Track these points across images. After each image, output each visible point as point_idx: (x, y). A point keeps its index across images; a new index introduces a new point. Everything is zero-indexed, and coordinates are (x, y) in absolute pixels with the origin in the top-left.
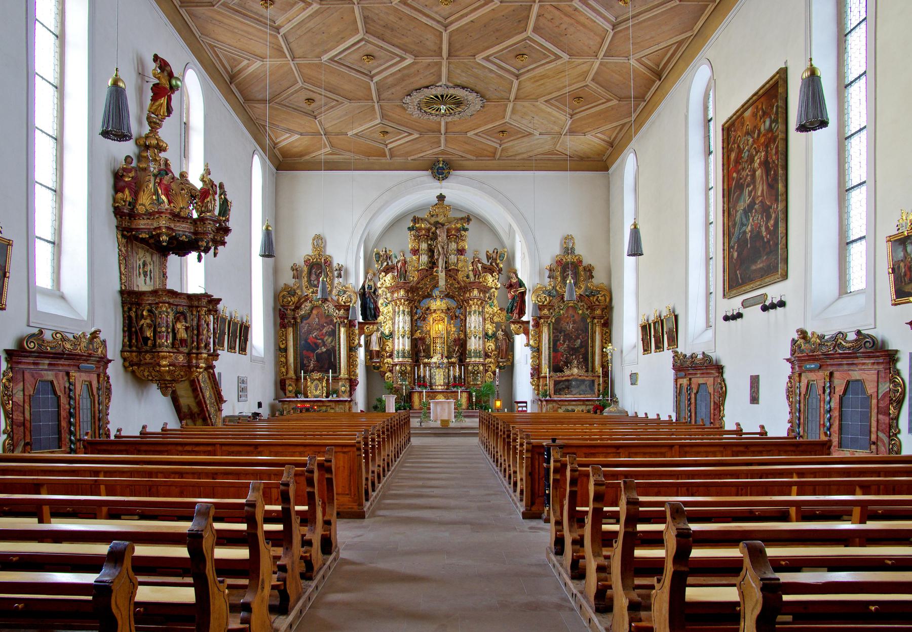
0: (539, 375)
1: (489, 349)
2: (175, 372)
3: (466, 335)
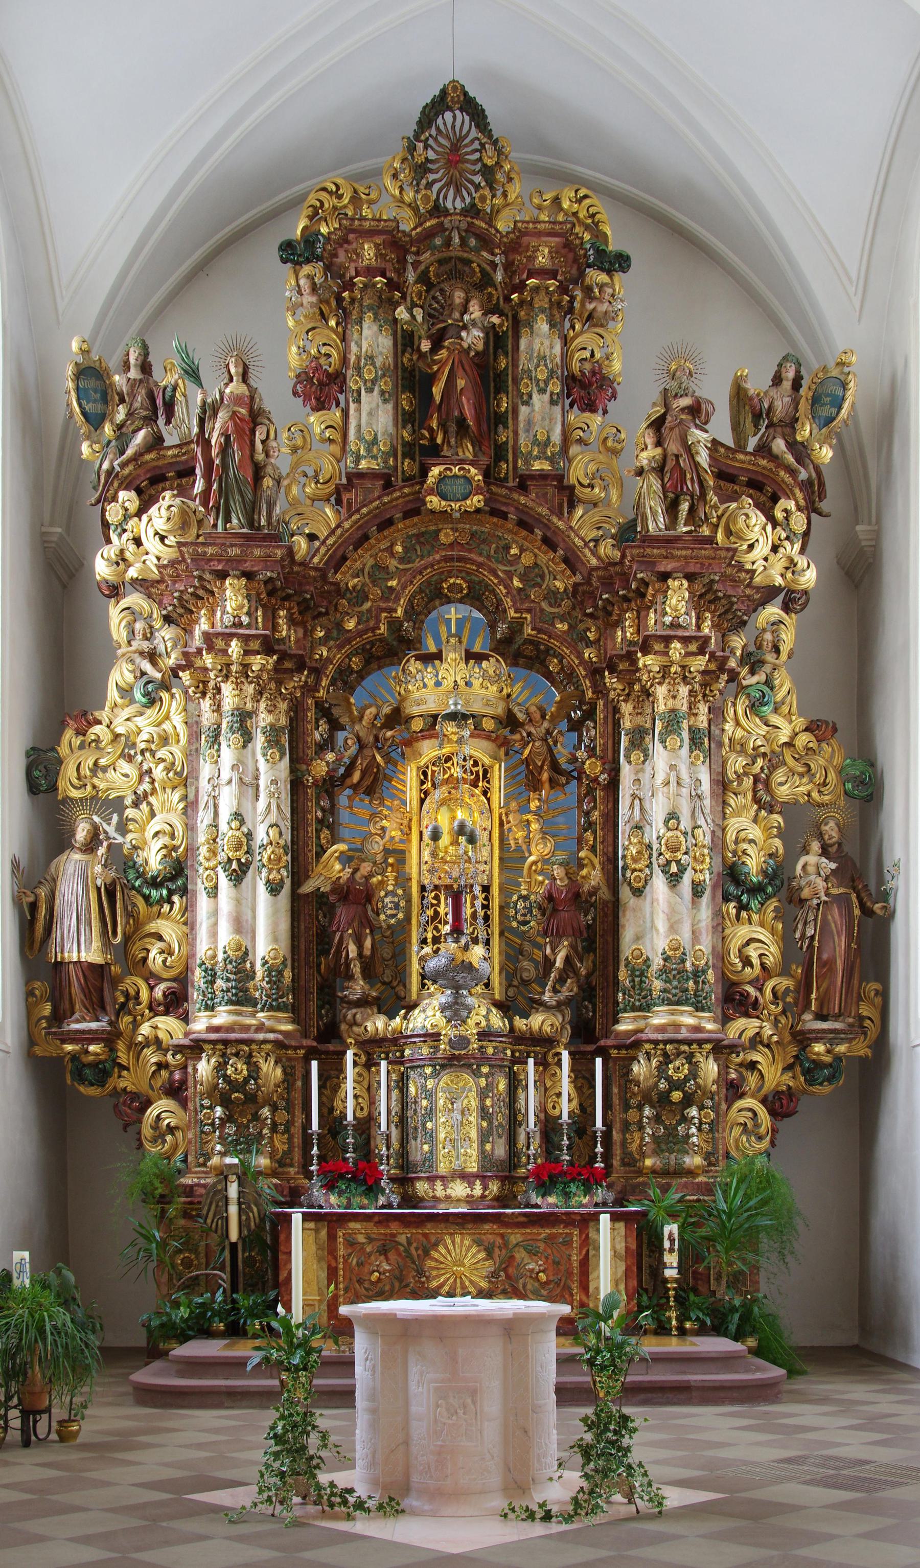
1: (747, 962)
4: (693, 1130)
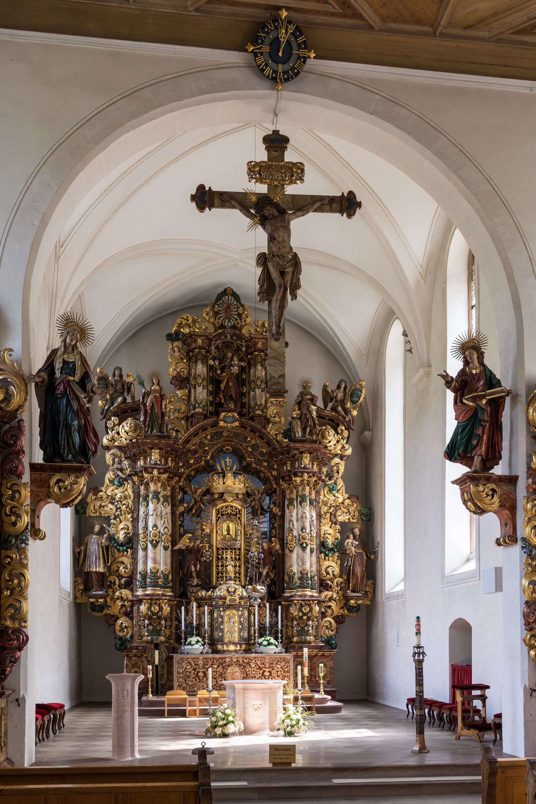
4: (310, 628)
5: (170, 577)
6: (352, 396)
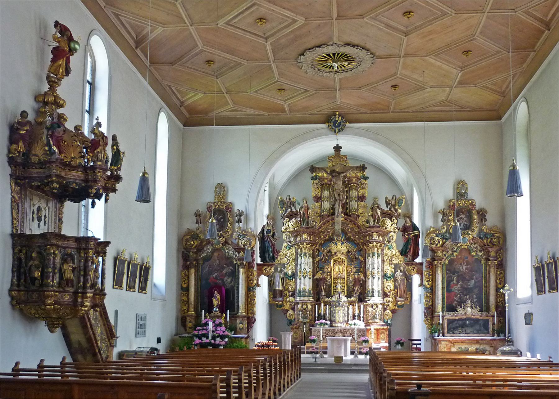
0: (432, 314)
2: (60, 310)
3: (365, 276)
5: (312, 291)
6: (398, 203)
